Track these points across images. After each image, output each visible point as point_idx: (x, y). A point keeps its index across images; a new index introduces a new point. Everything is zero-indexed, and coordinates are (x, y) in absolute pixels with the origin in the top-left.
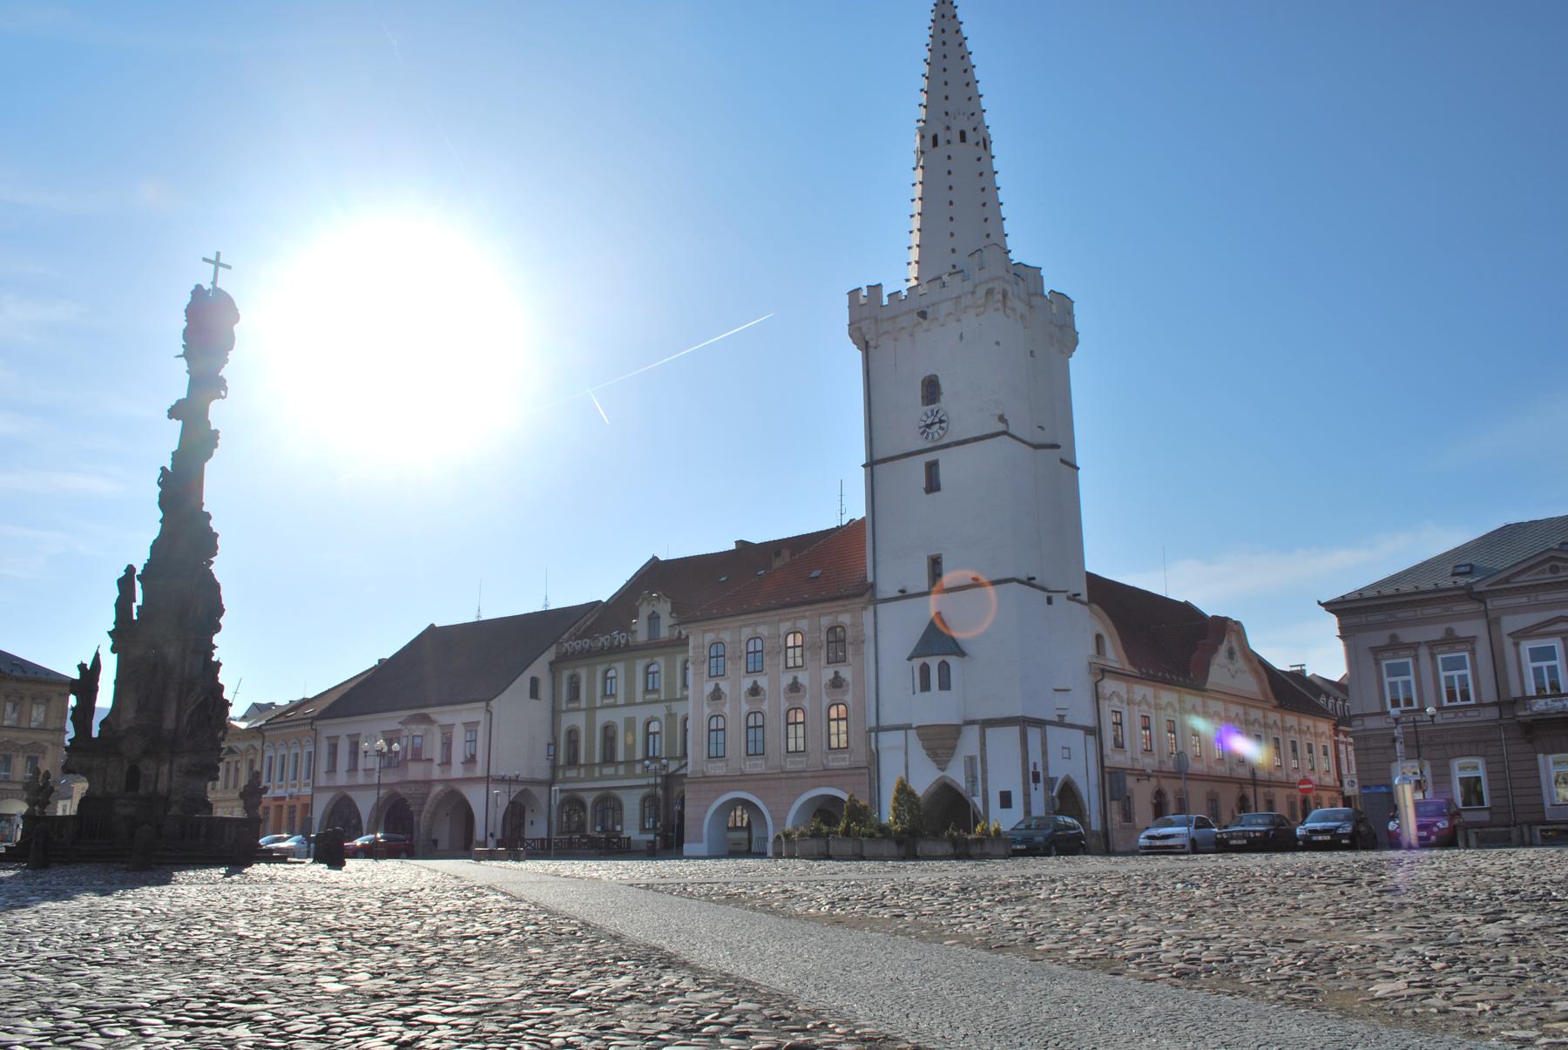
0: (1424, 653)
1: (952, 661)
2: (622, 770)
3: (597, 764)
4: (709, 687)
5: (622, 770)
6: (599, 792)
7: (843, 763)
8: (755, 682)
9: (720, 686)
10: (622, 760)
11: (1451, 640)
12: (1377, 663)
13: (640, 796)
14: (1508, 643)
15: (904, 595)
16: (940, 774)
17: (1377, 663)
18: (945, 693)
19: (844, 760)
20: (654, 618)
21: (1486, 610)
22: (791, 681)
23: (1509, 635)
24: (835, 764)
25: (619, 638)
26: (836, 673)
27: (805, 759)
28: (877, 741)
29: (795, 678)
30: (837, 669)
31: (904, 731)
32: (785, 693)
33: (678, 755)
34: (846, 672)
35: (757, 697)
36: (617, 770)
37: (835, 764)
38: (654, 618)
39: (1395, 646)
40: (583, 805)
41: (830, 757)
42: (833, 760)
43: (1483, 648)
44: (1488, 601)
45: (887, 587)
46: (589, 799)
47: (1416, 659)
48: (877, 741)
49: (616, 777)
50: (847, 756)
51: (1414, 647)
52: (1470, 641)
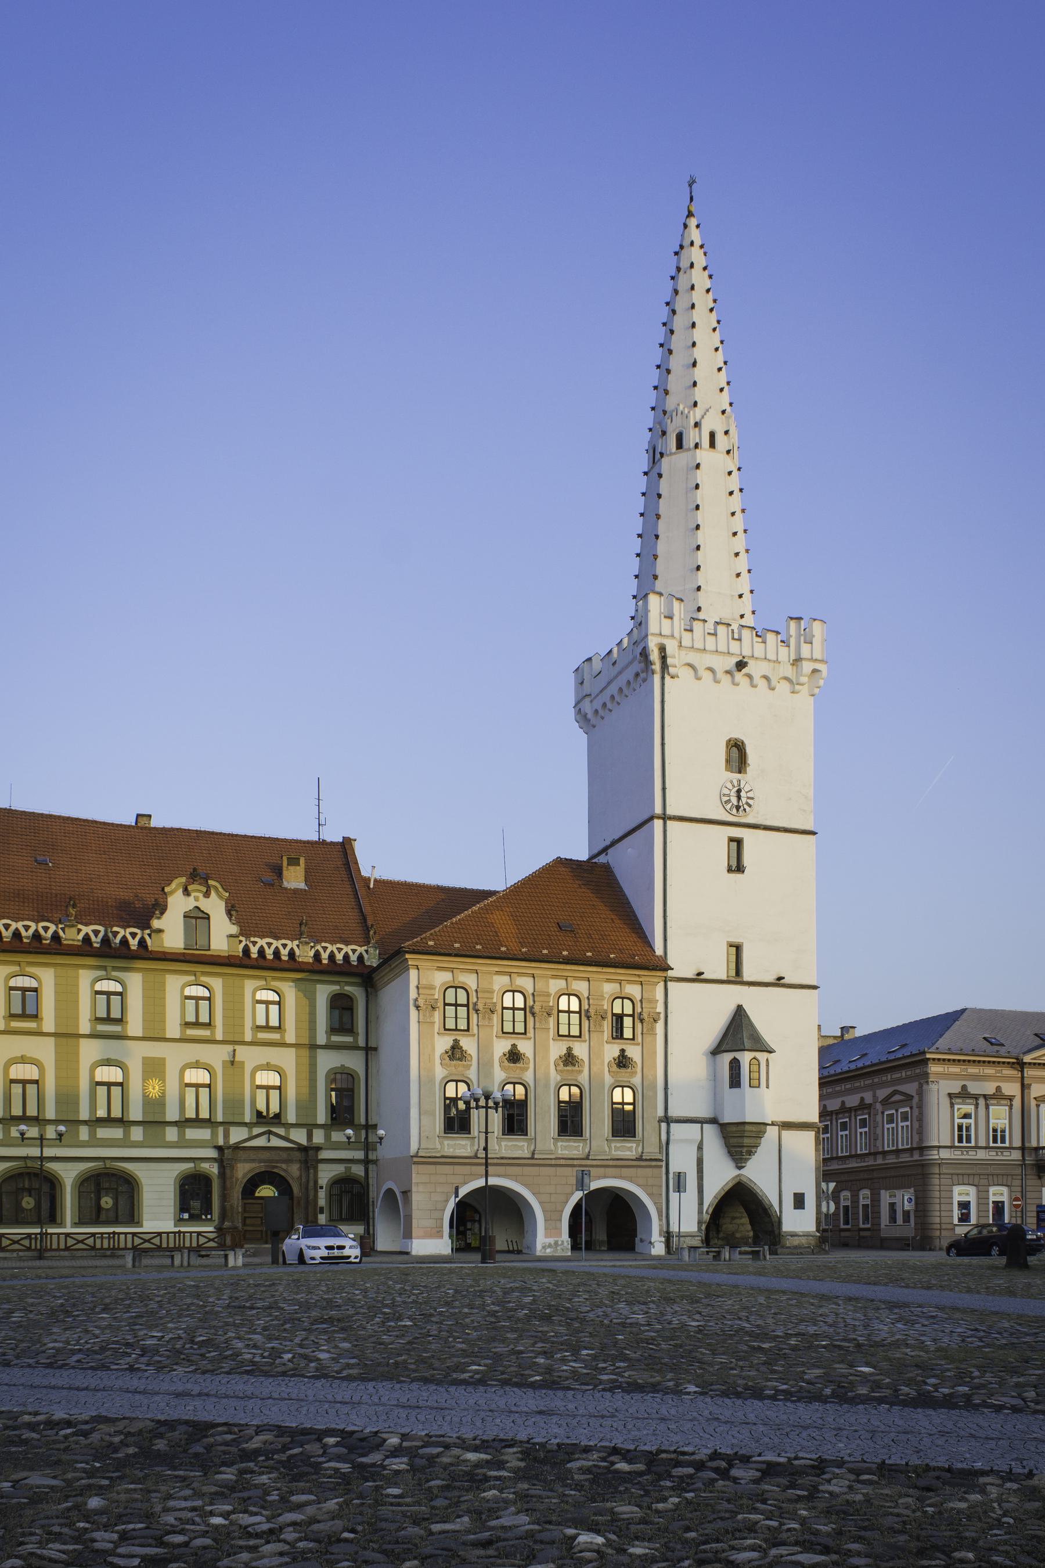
0: (982, 1102)
1: (762, 1056)
2: (137, 1134)
3: (85, 1122)
4: (443, 1043)
5: (137, 1134)
6: (100, 1164)
7: (628, 1153)
8: (514, 1046)
9: (461, 1043)
10: (139, 1118)
11: (998, 1096)
12: (952, 1105)
13: (176, 1173)
14: (1033, 1103)
15: (699, 978)
16: (737, 1172)
17: (952, 1105)
18: (735, 1090)
19: (630, 1149)
20: (197, 918)
21: (1023, 1078)
22: (565, 1051)
23: (1035, 1098)
24: (619, 1153)
25: (128, 934)
26: (623, 1051)
27: (581, 1145)
28: (668, 1133)
29: (569, 1049)
30: (624, 1047)
31: (699, 1125)
32: (501, 1062)
33: (247, 1120)
34: (634, 1052)
35: (518, 1065)
36: (127, 1134)
37: (619, 1153)
38: (197, 918)
39: (964, 1094)
40: (53, 1183)
41: (613, 1145)
42: (617, 1149)
43: (1017, 1103)
44: (1025, 1070)
45: (680, 964)
46: (68, 1175)
47: (977, 1106)
48: (668, 1133)
49: (125, 1142)
50: (634, 1145)
51: (976, 1097)
52: (1011, 1099)
